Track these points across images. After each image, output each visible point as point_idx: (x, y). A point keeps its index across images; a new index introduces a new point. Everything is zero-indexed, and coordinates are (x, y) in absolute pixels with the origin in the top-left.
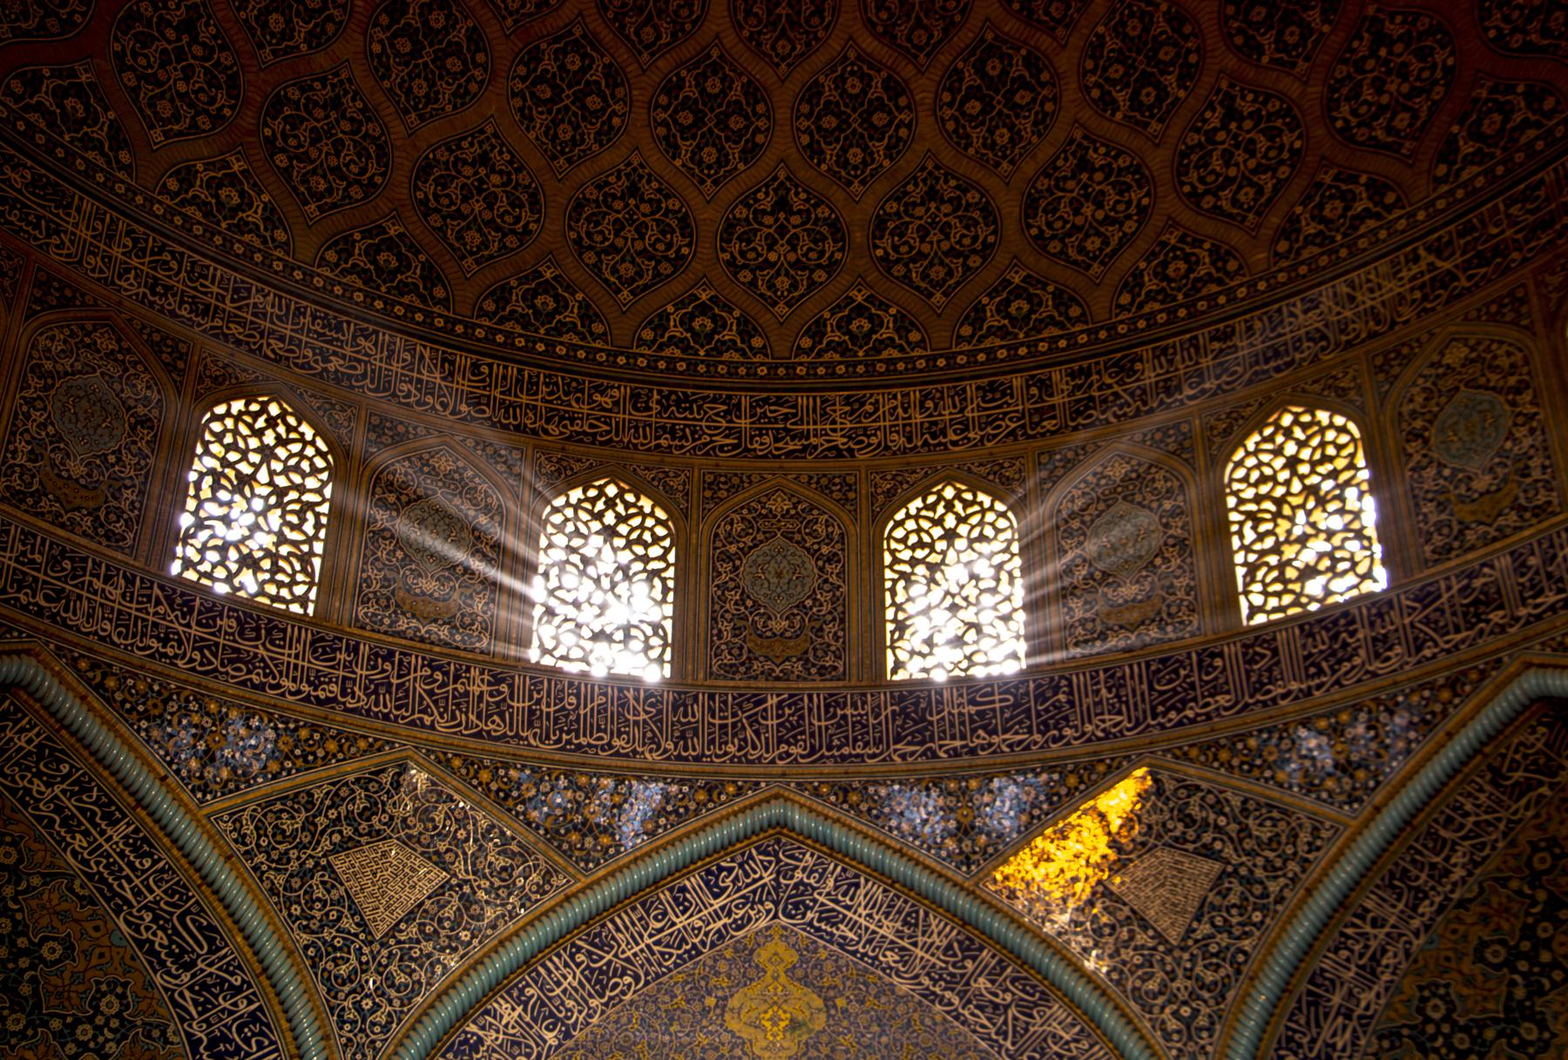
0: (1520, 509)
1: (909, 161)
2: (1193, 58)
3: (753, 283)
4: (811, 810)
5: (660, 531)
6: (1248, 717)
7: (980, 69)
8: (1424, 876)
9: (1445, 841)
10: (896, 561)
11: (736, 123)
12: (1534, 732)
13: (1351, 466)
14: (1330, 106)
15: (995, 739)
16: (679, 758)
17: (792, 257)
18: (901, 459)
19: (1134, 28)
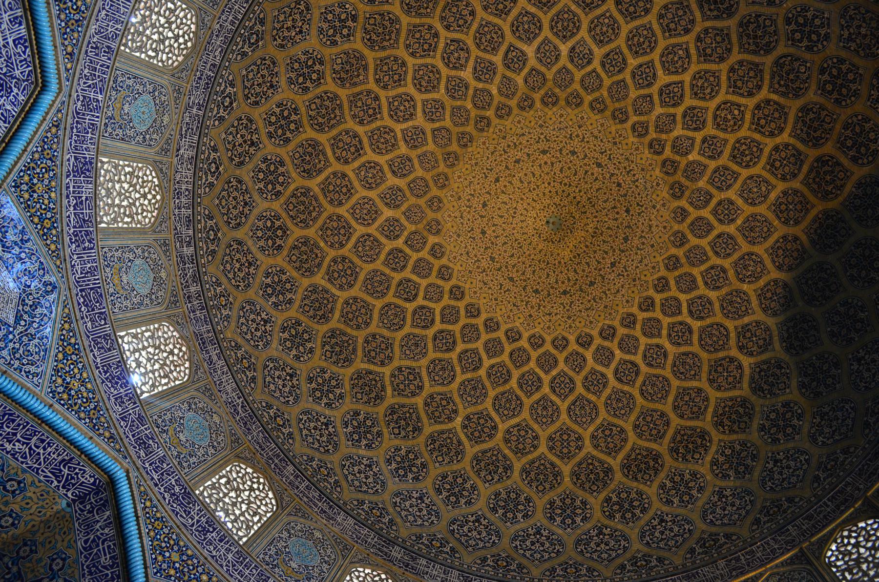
0: (178, 456)
1: (256, 196)
2: (280, 307)
3: (233, 126)
4: (51, 106)
5: (170, 62)
6: (84, 338)
7: (280, 228)
8: (9, 430)
9: (30, 439)
10: (140, 169)
11: (280, 132)
12: (90, 476)
13: (176, 379)
14: (270, 359)
15: (72, 208)
16: (89, 43)
17: (237, 144)
18: (173, 177)
19: (288, 286)
